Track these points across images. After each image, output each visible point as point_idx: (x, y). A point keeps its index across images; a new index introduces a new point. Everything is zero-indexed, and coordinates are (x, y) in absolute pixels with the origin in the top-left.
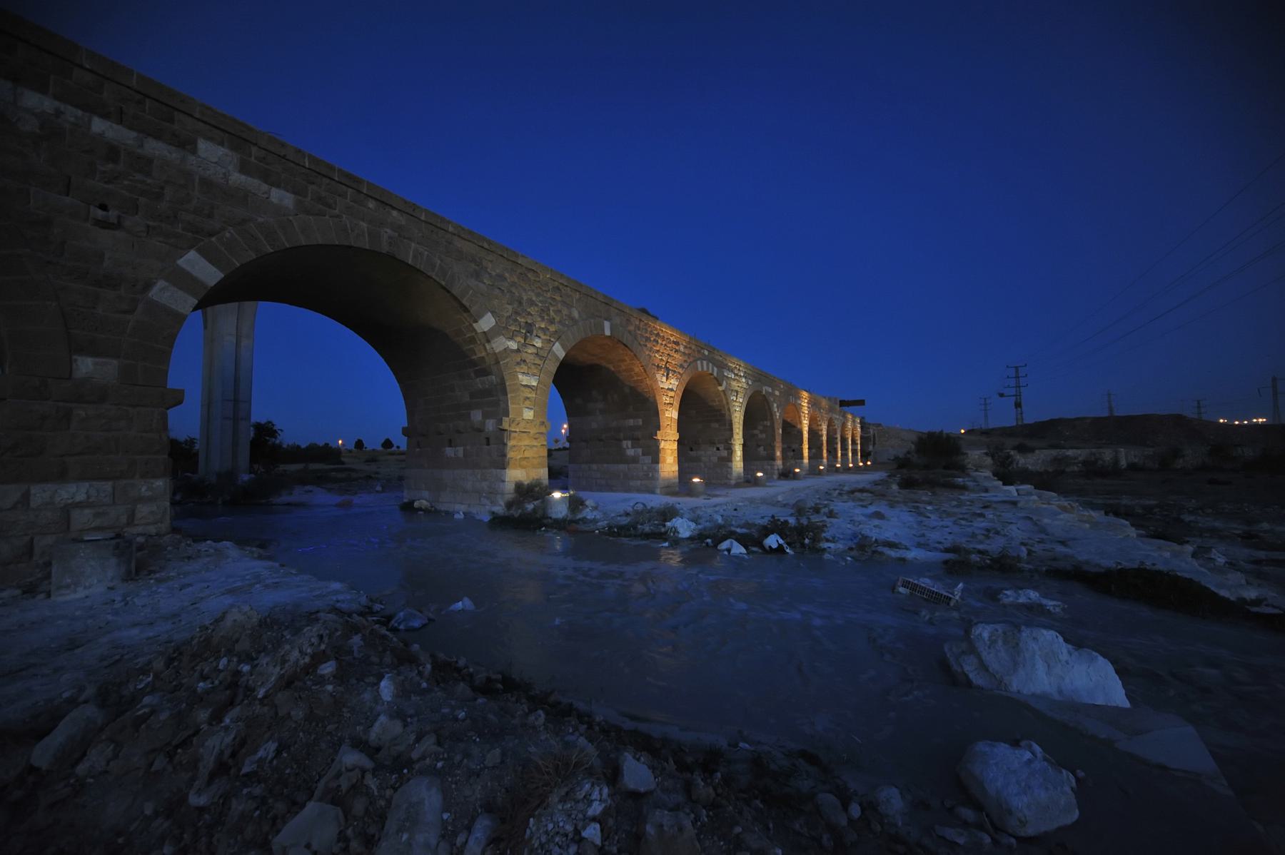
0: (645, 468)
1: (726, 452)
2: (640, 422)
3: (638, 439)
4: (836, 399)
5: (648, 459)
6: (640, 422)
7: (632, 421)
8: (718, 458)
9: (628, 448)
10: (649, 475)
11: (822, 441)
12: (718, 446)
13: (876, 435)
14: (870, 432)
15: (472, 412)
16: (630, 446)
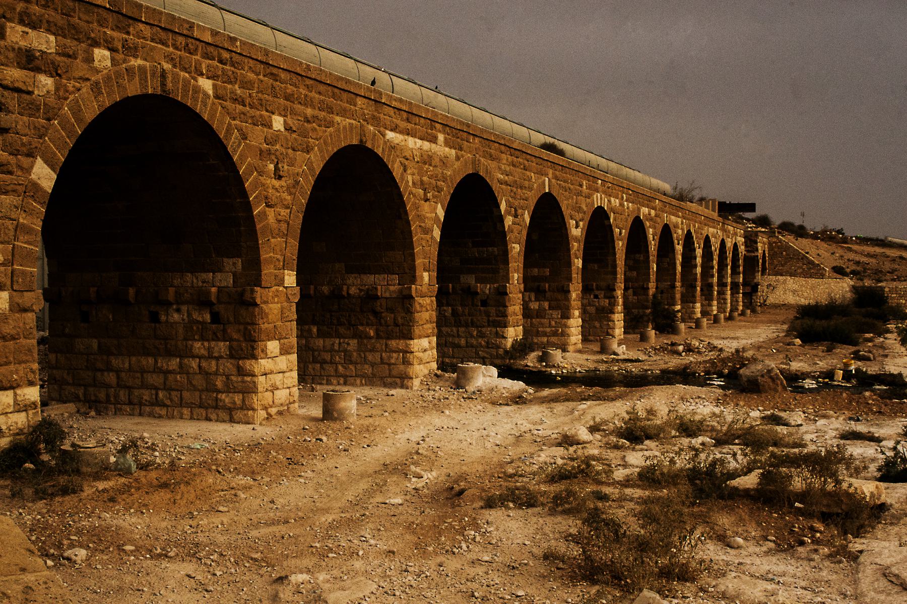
0: (553, 323)
1: (607, 301)
2: (547, 272)
3: (545, 291)
4: (714, 201)
5: (556, 314)
6: (547, 272)
7: (536, 270)
8: (597, 309)
9: (531, 301)
10: (558, 330)
11: (696, 274)
12: (597, 293)
13: (767, 252)
14: (757, 250)
15: (461, 276)
16: (533, 299)
